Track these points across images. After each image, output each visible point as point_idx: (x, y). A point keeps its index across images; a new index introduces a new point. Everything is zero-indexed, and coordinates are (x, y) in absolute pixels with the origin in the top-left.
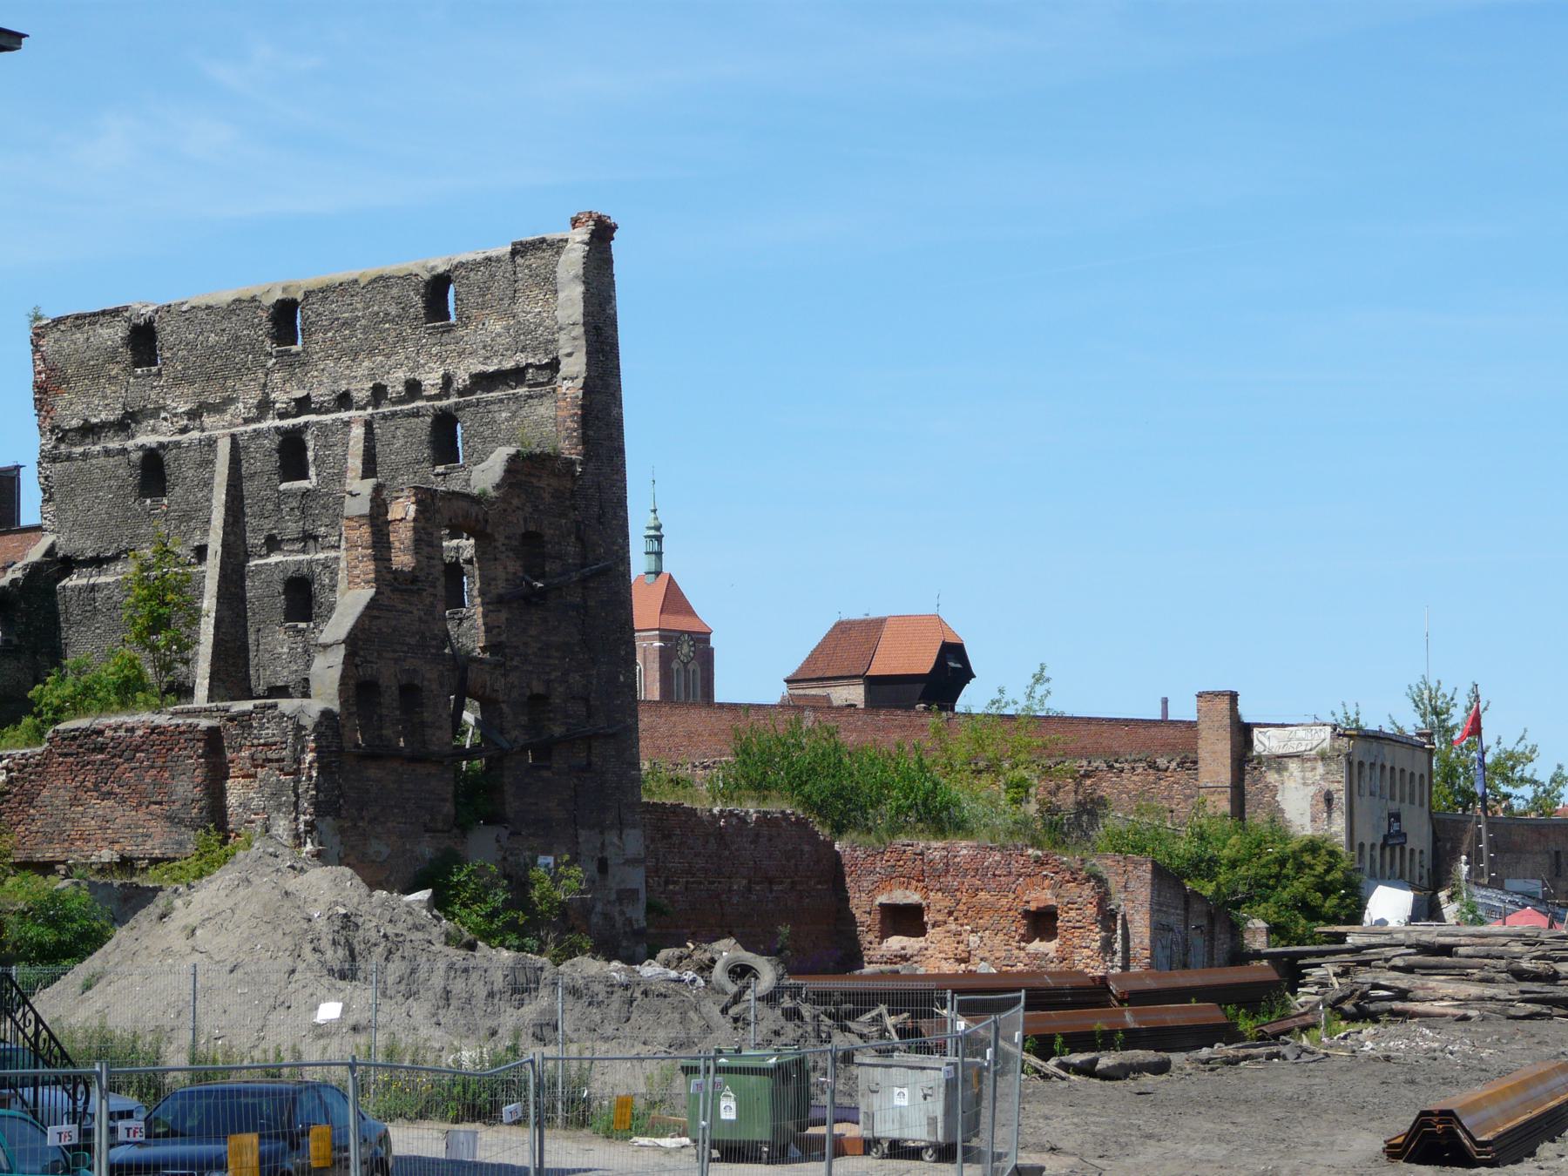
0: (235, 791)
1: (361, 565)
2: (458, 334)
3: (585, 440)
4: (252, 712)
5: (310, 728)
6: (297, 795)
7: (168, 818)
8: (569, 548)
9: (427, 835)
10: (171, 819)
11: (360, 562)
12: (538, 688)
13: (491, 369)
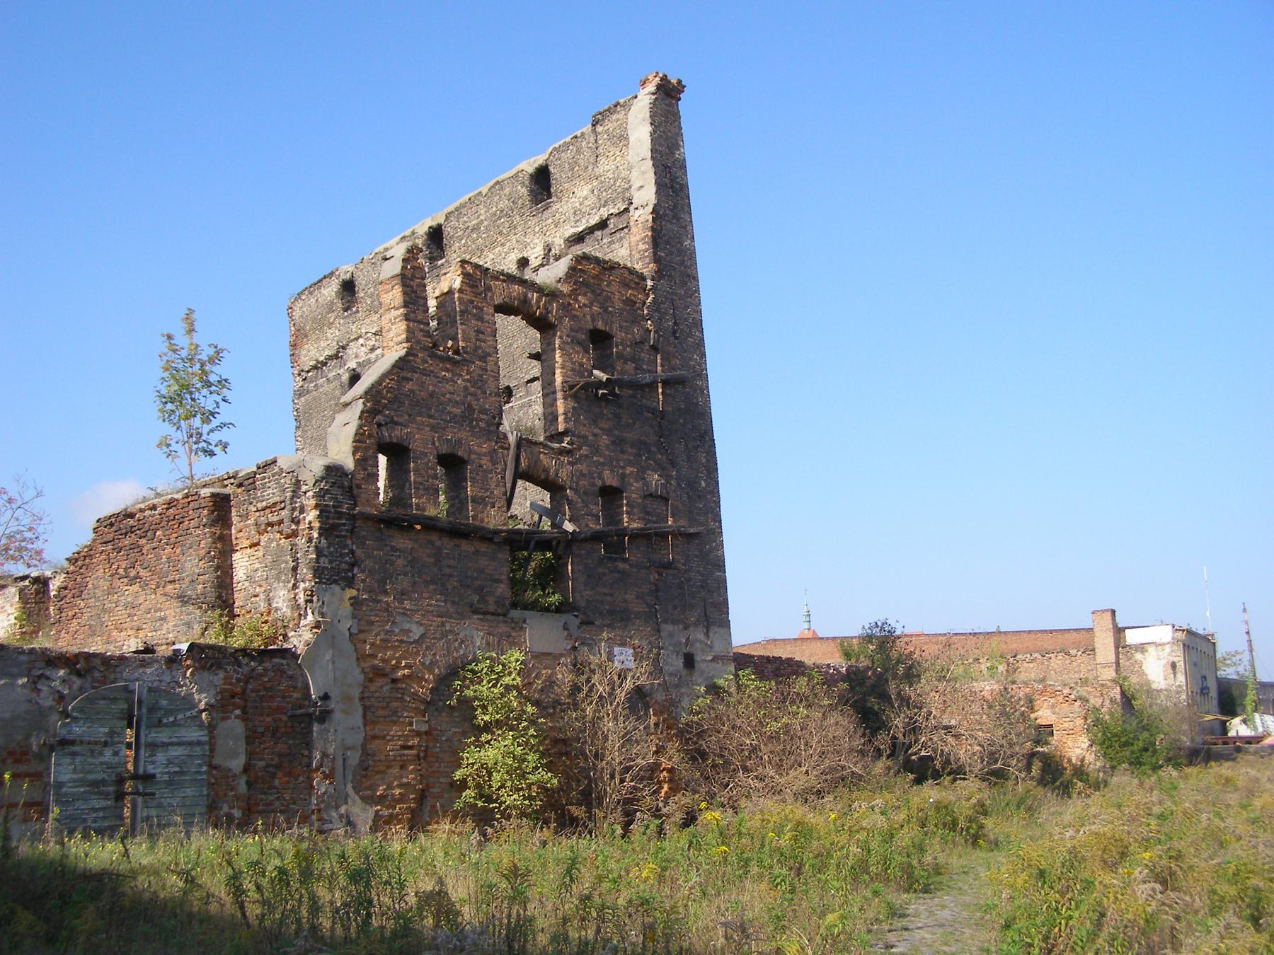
0: (242, 564)
1: (393, 327)
2: (554, 208)
3: (656, 259)
4: (255, 473)
5: (311, 483)
6: (296, 560)
7: (178, 597)
8: (643, 355)
9: (476, 617)
10: (183, 599)
11: (392, 324)
12: (610, 480)
13: (580, 229)
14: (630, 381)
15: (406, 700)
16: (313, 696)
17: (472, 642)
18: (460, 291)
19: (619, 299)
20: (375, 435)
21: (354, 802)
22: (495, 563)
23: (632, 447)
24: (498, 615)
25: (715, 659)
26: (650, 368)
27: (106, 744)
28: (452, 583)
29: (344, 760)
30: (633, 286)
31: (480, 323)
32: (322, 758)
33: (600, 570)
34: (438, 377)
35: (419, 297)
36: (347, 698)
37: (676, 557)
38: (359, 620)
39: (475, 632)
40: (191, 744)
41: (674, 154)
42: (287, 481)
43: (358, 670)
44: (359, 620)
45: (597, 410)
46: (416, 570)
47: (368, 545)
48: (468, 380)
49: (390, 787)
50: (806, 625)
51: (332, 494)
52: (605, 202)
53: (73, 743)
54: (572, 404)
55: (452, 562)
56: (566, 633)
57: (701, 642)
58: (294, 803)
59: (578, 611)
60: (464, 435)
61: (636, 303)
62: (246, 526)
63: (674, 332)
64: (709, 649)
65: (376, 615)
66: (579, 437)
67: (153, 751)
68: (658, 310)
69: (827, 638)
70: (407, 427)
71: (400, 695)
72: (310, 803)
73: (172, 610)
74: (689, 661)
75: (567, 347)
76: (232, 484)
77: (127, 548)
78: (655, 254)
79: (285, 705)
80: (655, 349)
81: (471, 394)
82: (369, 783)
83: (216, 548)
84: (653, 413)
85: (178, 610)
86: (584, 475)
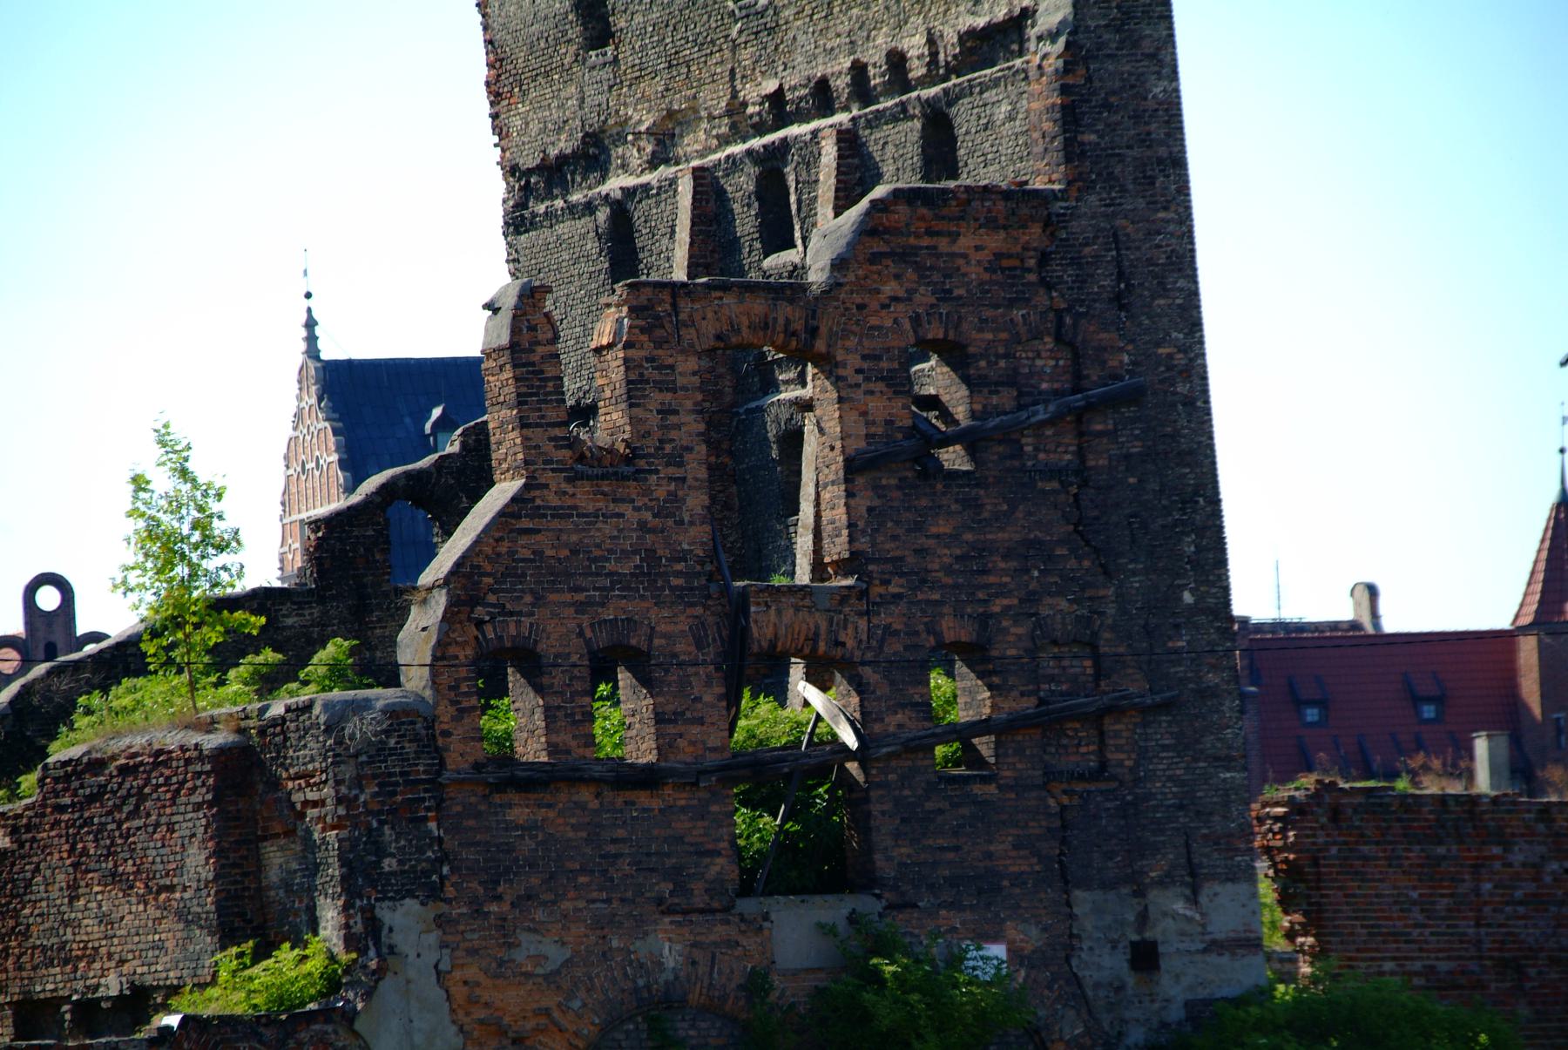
8: (1039, 362)
9: (667, 920)
22: (706, 824)
24: (713, 911)
26: (1056, 386)
38: (453, 950)
44: (453, 950)
46: (553, 854)
57: (1175, 916)
86: (896, 633)
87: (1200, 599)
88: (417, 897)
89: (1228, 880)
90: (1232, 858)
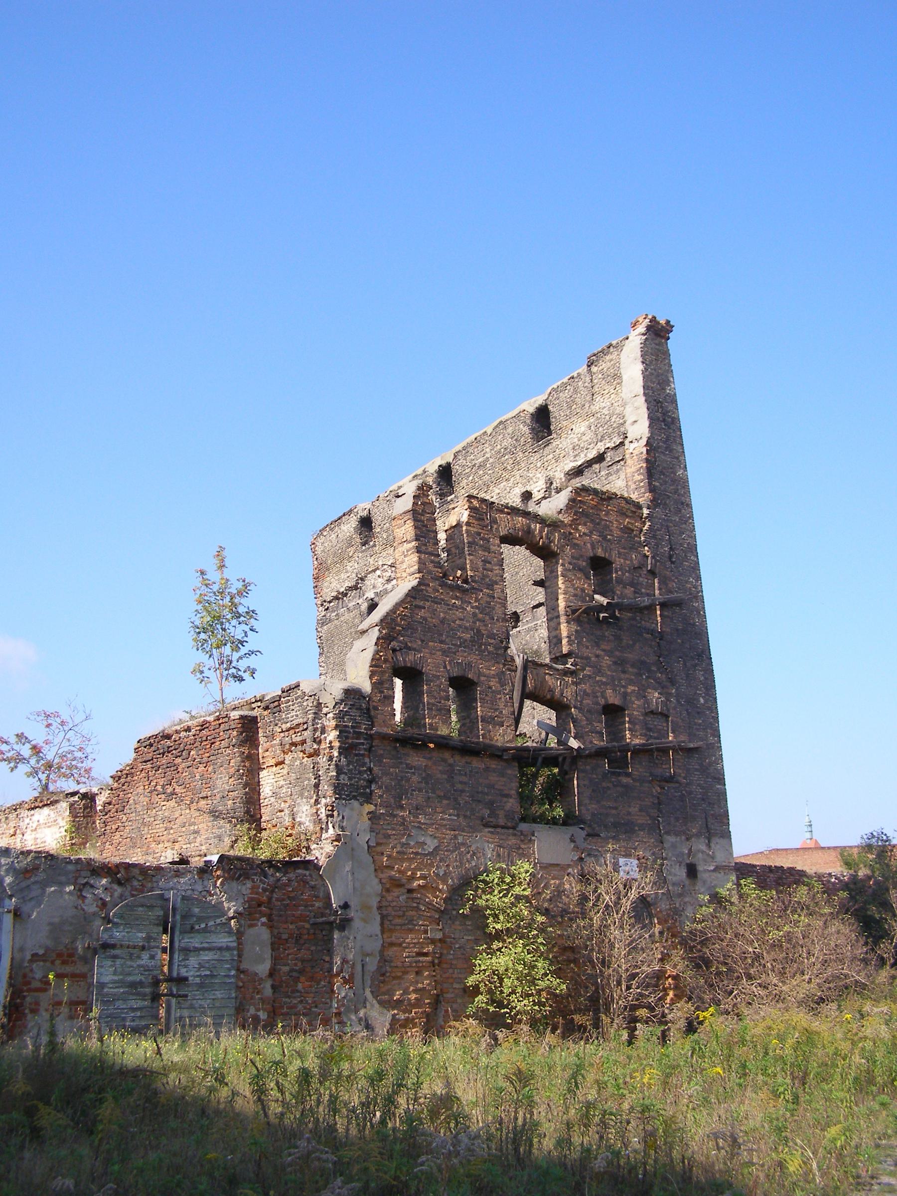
0: (268, 781)
1: (406, 559)
2: (554, 444)
3: (652, 489)
4: (280, 697)
5: (331, 705)
6: (318, 777)
8: (641, 579)
9: (487, 830)
10: (215, 814)
11: (405, 556)
12: (613, 698)
13: (579, 463)
14: (629, 605)
15: (421, 910)
16: (334, 905)
17: (484, 854)
18: (468, 524)
19: (617, 527)
20: (390, 660)
21: (372, 1006)
22: (505, 779)
23: (633, 666)
24: (508, 828)
25: (717, 869)
26: (648, 591)
27: (143, 948)
28: (464, 799)
29: (363, 966)
30: (630, 515)
31: (486, 554)
32: (342, 963)
33: (604, 784)
34: (448, 605)
35: (429, 531)
36: (365, 907)
37: (677, 771)
38: (377, 834)
39: (486, 844)
40: (220, 949)
41: (664, 389)
42: (309, 703)
43: (376, 881)
45: (599, 633)
46: (430, 786)
47: (385, 763)
48: (477, 607)
49: (406, 992)
50: (808, 835)
51: (351, 716)
52: (602, 437)
53: (113, 946)
54: (574, 627)
55: (464, 779)
56: (572, 845)
57: (703, 852)
58: (316, 1007)
59: (584, 822)
60: (473, 658)
61: (633, 530)
62: (272, 746)
63: (670, 557)
64: (711, 860)
65: (393, 829)
66: (582, 658)
67: (186, 955)
68: (654, 537)
69: (829, 848)
70: (420, 652)
71: (415, 905)
72: (331, 1007)
73: (204, 824)
74: (692, 871)
75: (570, 574)
76: (259, 707)
77: (165, 767)
78: (650, 484)
79: (308, 913)
80: (652, 573)
81: (479, 620)
82: (387, 987)
83: (245, 766)
84: (652, 635)
85: (210, 824)
87: (706, 701)
88: (358, 800)
89: (721, 837)
90: (722, 826)
